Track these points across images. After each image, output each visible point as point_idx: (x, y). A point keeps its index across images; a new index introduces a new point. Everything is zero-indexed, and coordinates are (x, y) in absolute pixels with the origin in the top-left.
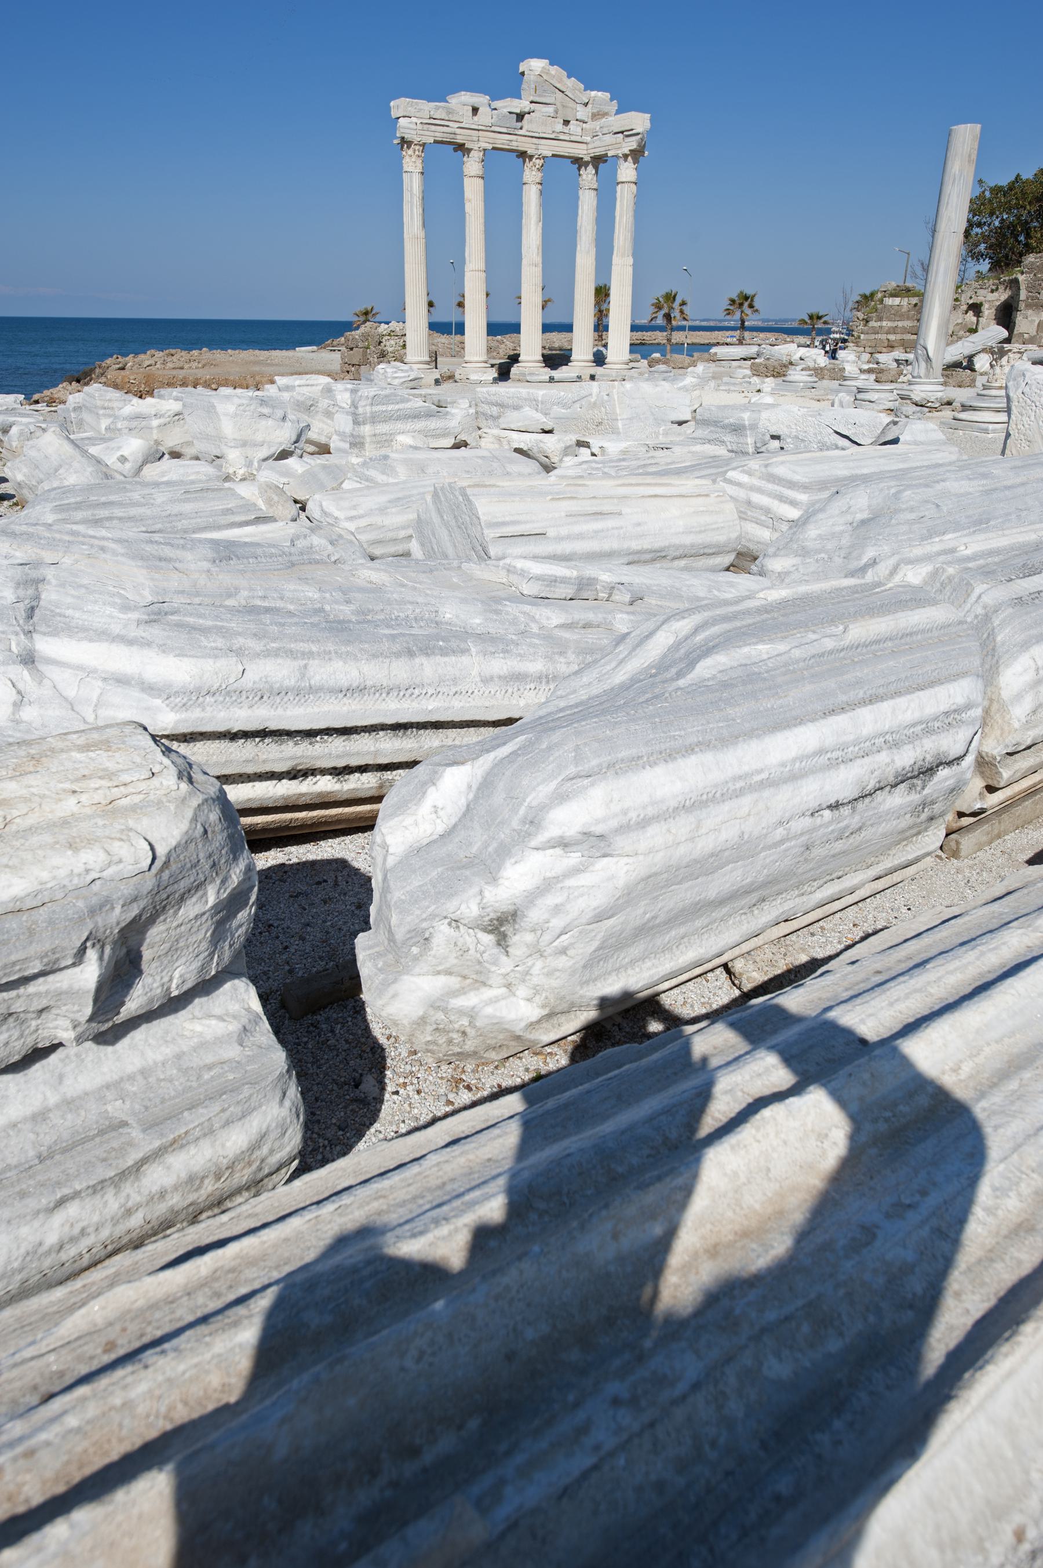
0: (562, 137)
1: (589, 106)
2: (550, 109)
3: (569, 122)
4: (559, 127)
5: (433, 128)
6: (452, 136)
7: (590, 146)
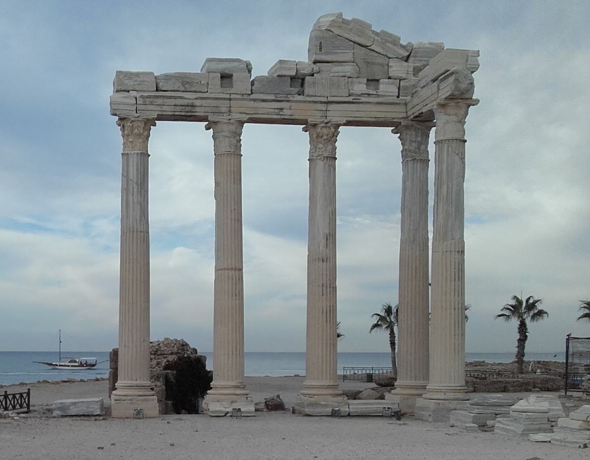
0: (363, 99)
1: (411, 59)
2: (348, 69)
3: (378, 81)
4: (360, 87)
5: (159, 101)
6: (188, 109)
7: (409, 106)
